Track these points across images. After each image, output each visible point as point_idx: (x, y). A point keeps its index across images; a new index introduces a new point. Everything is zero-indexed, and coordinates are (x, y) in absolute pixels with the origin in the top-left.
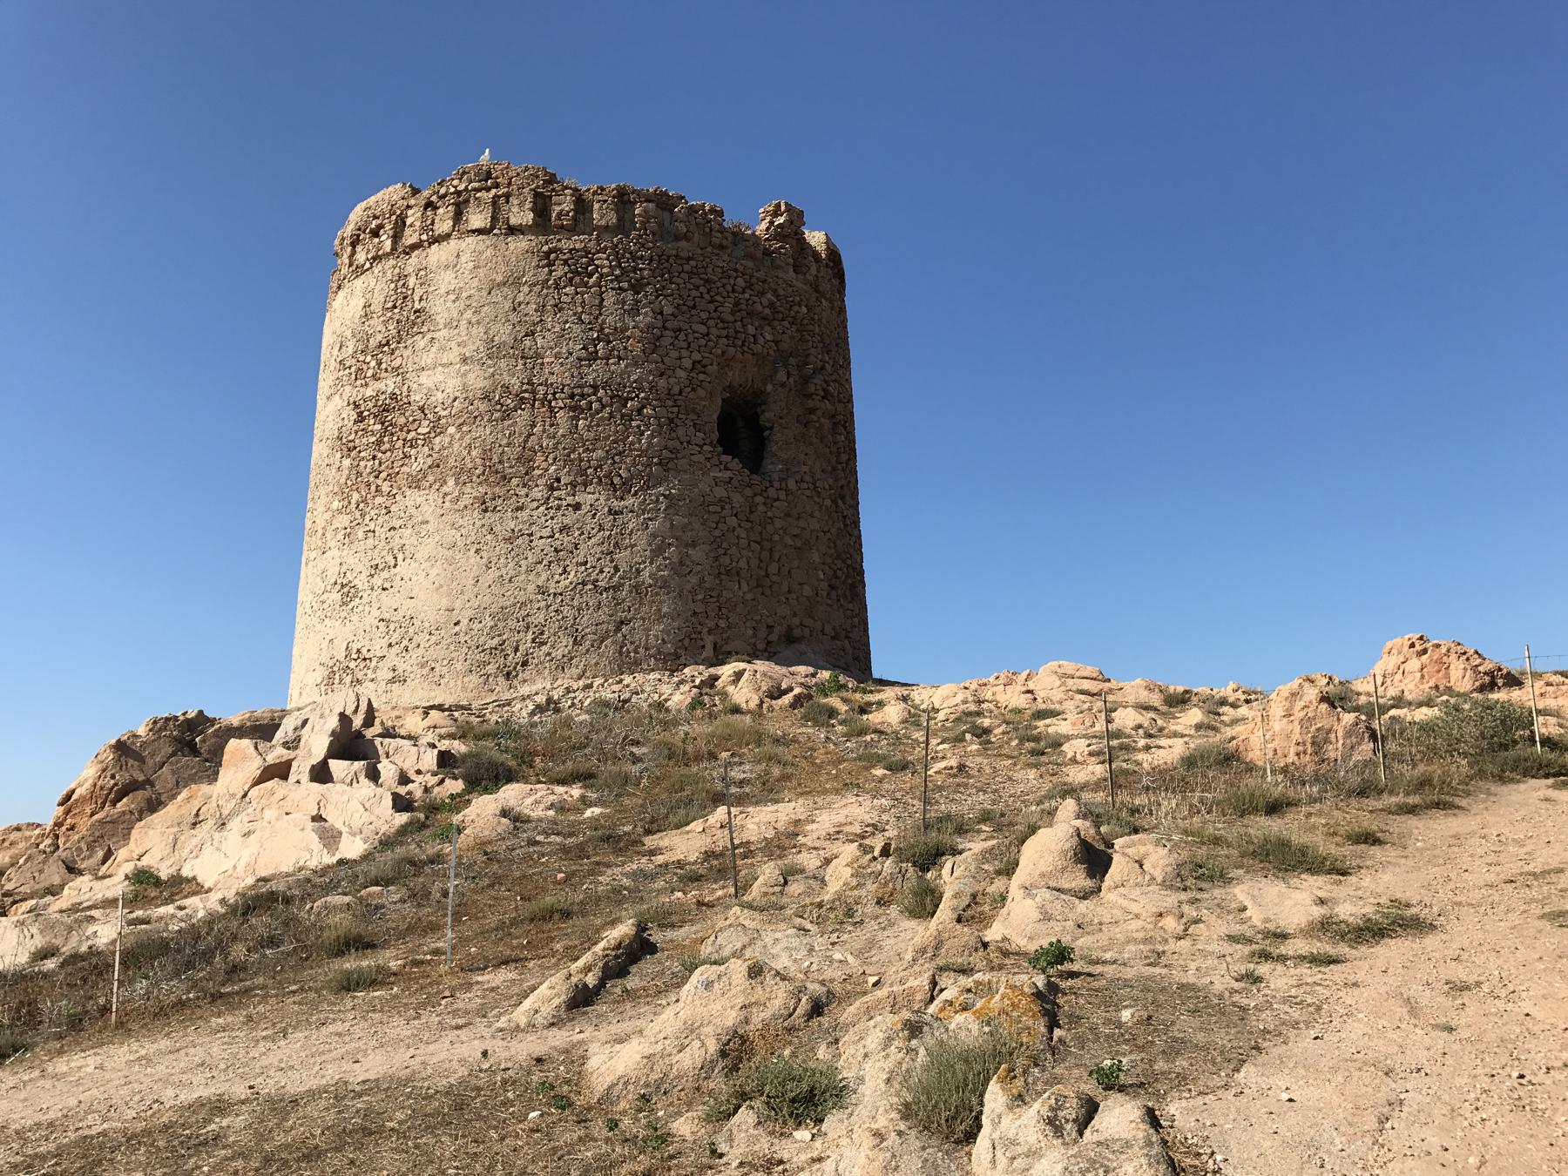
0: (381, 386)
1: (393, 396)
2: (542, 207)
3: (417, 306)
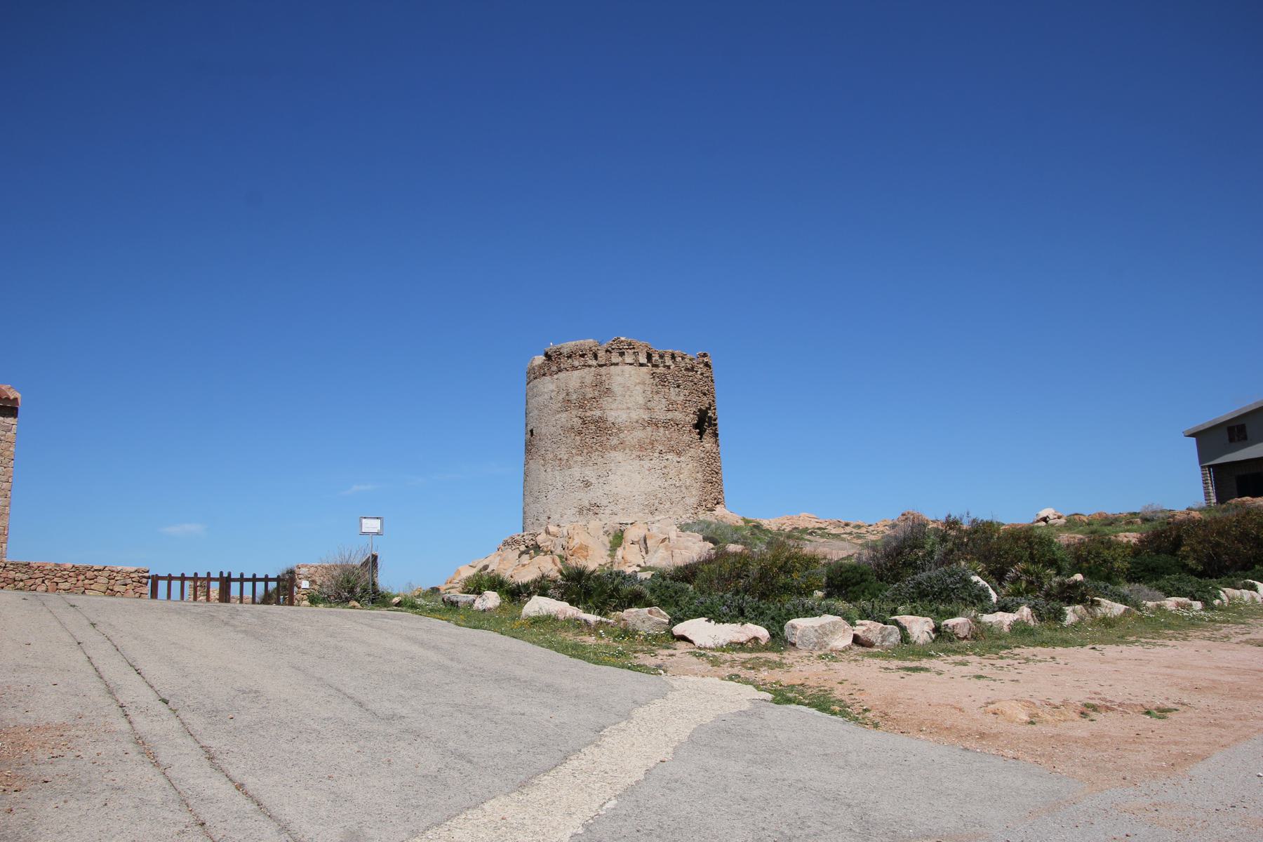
2: (649, 357)
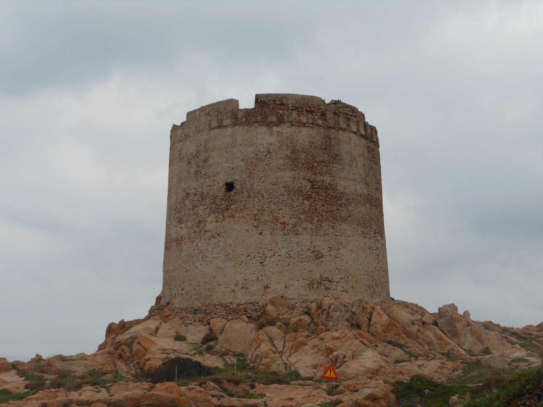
0: (322, 178)
1: (330, 184)
3: (336, 152)
